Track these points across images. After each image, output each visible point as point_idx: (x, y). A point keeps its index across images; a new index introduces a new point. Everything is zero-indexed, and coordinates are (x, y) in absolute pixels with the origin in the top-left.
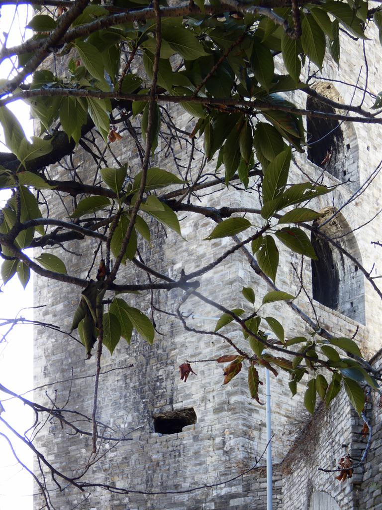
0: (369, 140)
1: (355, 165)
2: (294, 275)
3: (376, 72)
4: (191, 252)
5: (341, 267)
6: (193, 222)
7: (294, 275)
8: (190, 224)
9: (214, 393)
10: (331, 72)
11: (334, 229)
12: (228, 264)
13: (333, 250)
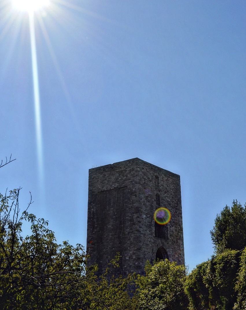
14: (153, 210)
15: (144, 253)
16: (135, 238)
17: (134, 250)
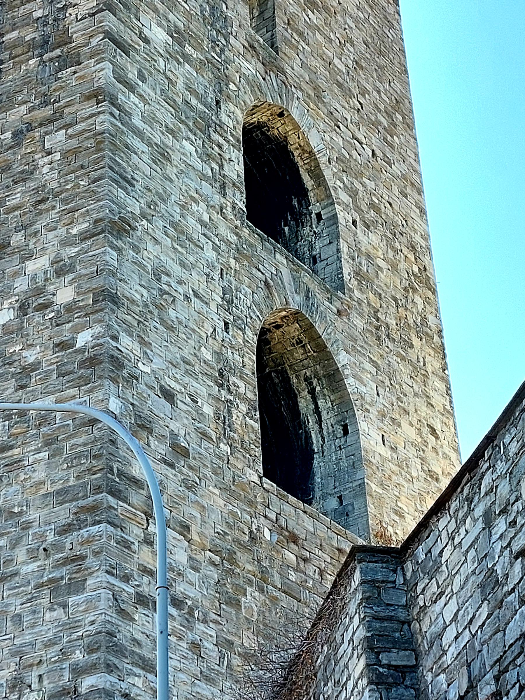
0: (355, 210)
1: (333, 247)
2: (224, 423)
3: (360, 108)
4: (9, 358)
5: (316, 427)
6: (17, 301)
7: (224, 423)
8: (11, 303)
9: (43, 669)
10: (284, 92)
11: (299, 354)
12: (86, 385)
13: (300, 392)
16: (76, 152)
17: (66, 242)
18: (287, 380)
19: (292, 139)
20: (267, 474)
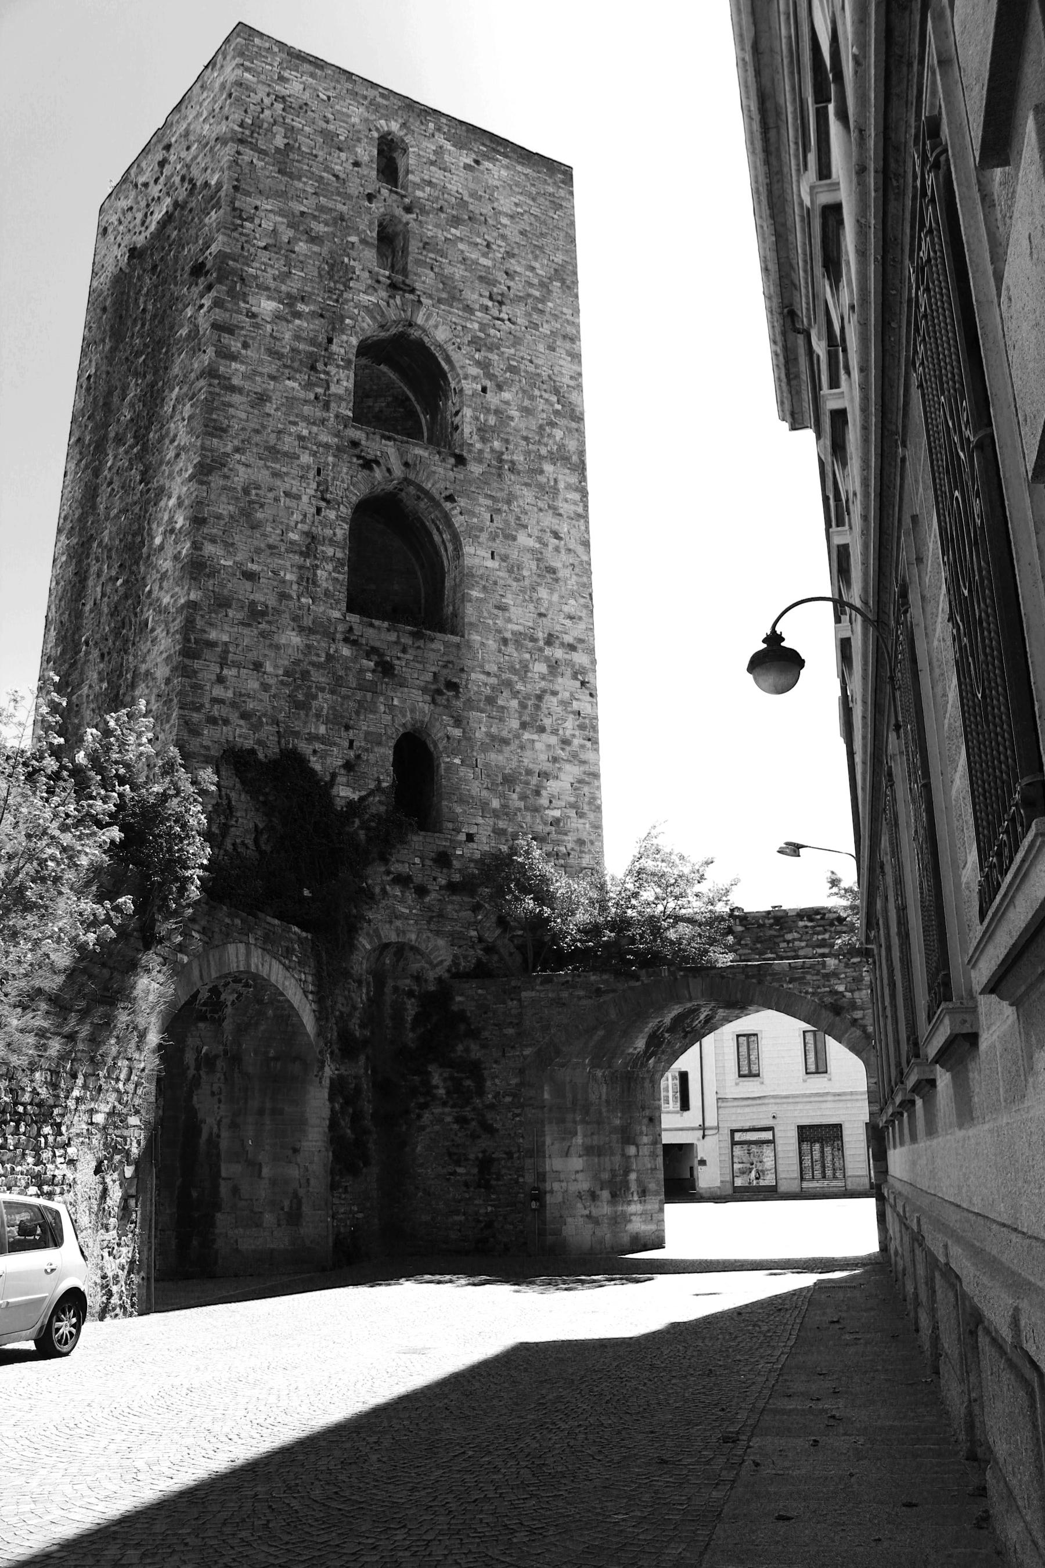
14: (348, 288)
15: (246, 491)
18: (423, 524)
19: (426, 339)
20: (350, 609)
